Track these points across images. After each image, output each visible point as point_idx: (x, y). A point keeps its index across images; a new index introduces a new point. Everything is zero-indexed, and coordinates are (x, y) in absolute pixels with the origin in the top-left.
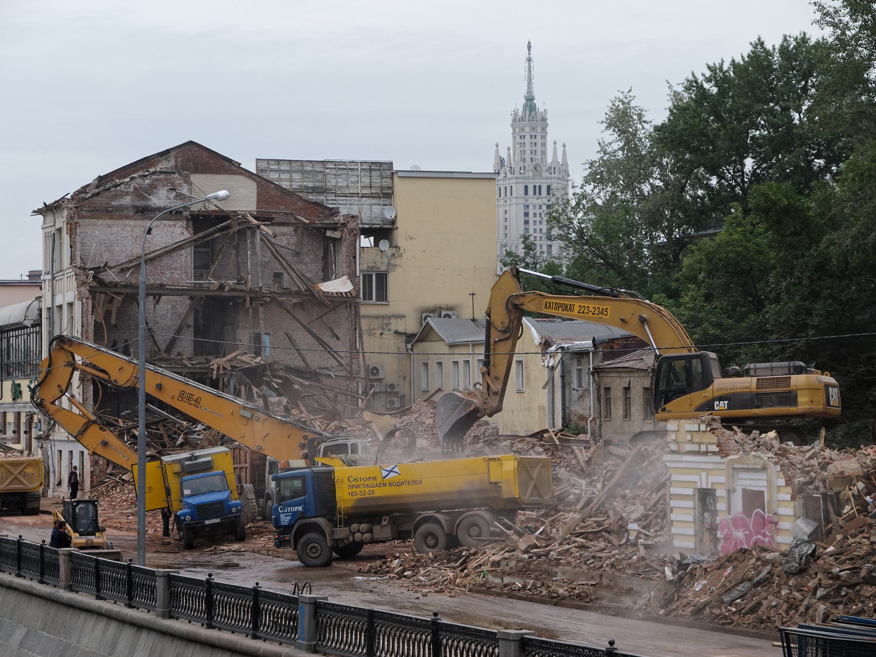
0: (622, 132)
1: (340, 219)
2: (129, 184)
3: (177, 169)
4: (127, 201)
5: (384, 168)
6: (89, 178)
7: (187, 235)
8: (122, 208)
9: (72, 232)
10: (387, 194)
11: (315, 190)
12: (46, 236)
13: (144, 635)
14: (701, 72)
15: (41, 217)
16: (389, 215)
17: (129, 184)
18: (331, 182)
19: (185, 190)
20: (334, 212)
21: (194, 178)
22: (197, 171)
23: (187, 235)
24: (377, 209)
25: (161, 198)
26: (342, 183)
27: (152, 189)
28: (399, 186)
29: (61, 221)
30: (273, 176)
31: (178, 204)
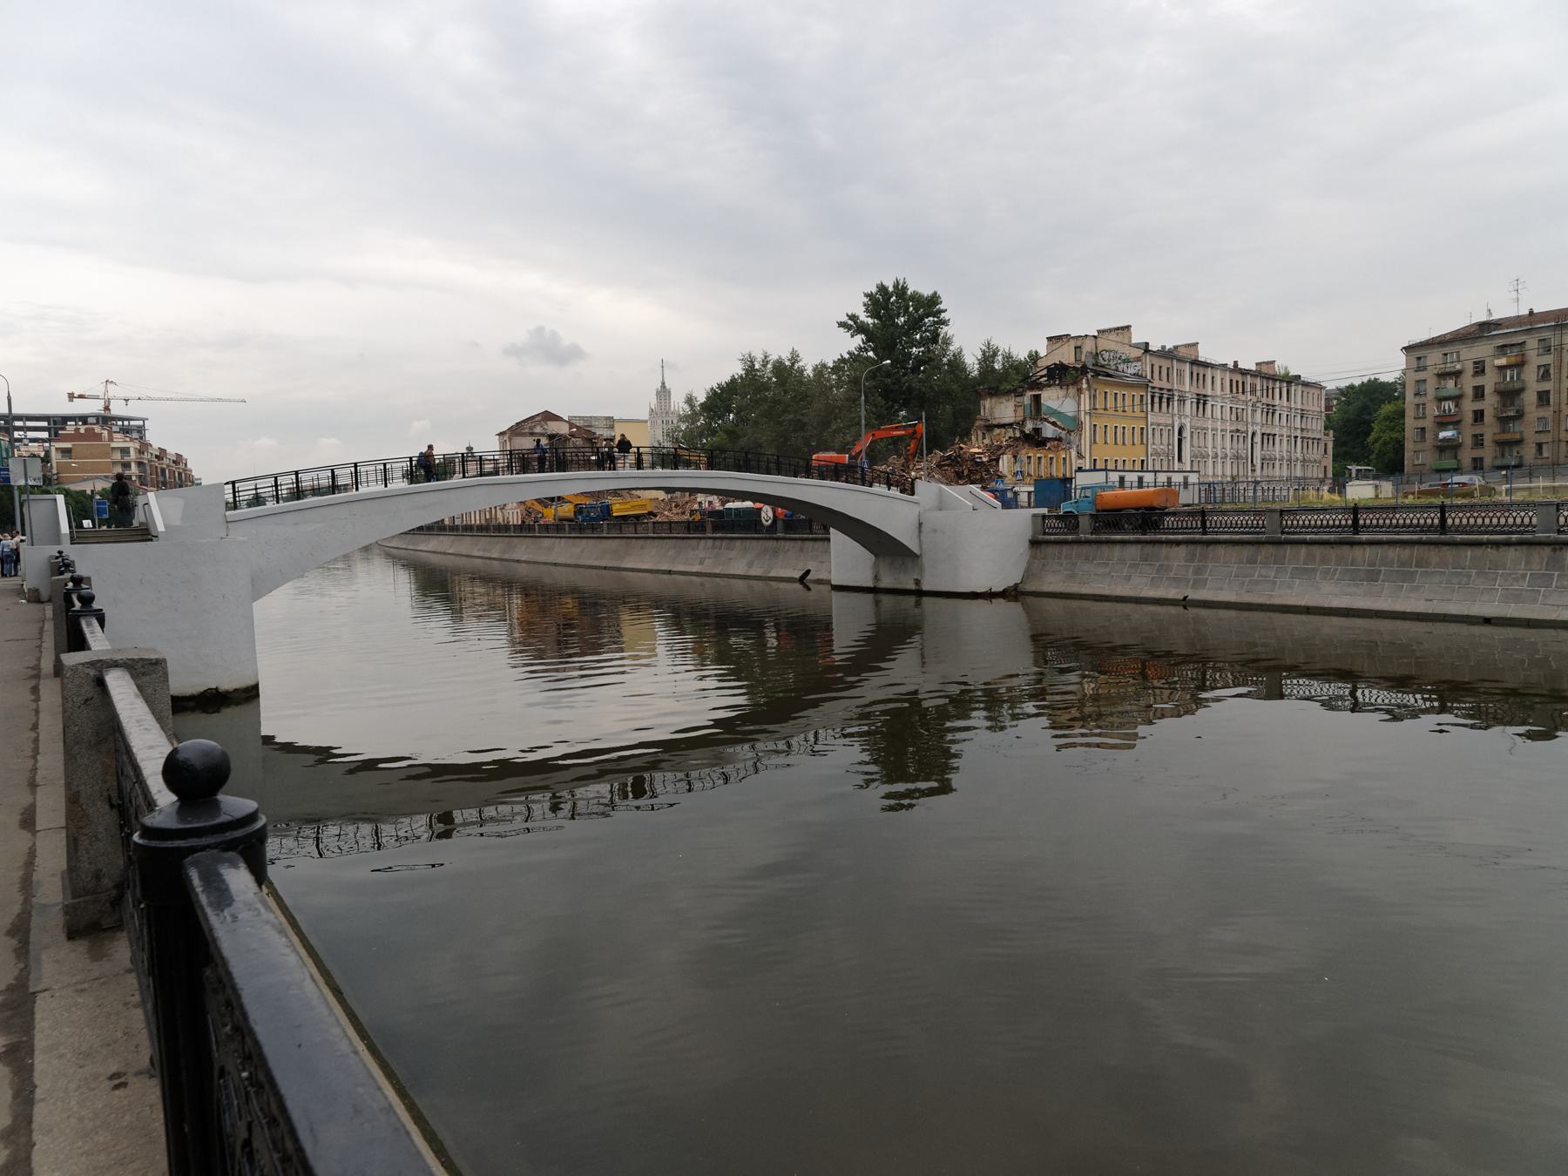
0: (690, 405)
1: (597, 436)
2: (527, 425)
3: (542, 420)
4: (527, 431)
5: (610, 419)
6: (513, 423)
7: (547, 442)
8: (524, 433)
9: (510, 441)
10: (612, 427)
11: (588, 426)
12: (500, 443)
13: (563, 540)
14: (715, 387)
15: (498, 437)
16: (613, 434)
17: (527, 425)
18: (593, 423)
19: (545, 427)
20: (595, 433)
21: (548, 423)
22: (550, 420)
23: (547, 442)
24: (608, 432)
25: (538, 430)
26: (597, 423)
27: (535, 427)
28: (616, 424)
29: (506, 438)
30: (574, 422)
31: (543, 431)
